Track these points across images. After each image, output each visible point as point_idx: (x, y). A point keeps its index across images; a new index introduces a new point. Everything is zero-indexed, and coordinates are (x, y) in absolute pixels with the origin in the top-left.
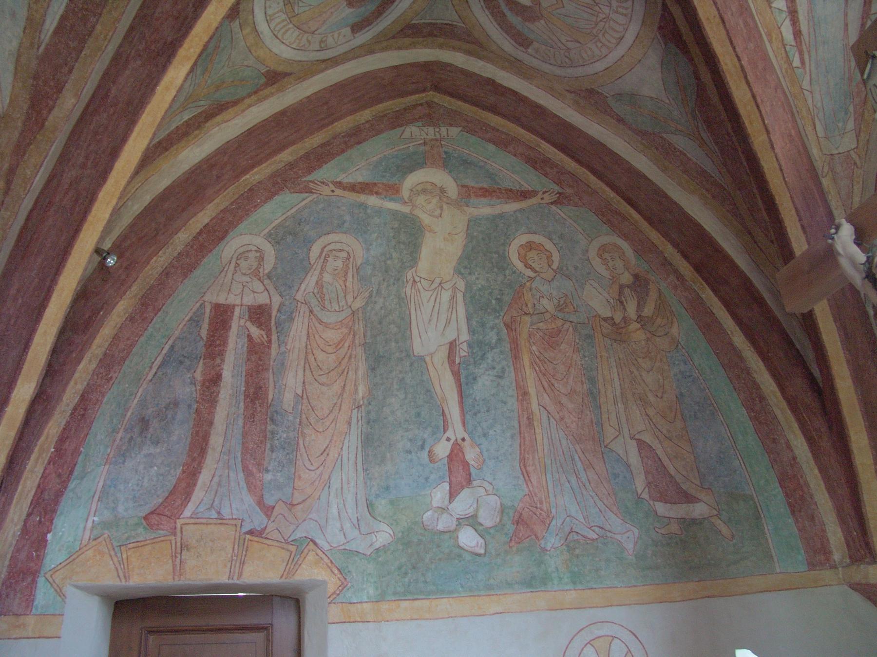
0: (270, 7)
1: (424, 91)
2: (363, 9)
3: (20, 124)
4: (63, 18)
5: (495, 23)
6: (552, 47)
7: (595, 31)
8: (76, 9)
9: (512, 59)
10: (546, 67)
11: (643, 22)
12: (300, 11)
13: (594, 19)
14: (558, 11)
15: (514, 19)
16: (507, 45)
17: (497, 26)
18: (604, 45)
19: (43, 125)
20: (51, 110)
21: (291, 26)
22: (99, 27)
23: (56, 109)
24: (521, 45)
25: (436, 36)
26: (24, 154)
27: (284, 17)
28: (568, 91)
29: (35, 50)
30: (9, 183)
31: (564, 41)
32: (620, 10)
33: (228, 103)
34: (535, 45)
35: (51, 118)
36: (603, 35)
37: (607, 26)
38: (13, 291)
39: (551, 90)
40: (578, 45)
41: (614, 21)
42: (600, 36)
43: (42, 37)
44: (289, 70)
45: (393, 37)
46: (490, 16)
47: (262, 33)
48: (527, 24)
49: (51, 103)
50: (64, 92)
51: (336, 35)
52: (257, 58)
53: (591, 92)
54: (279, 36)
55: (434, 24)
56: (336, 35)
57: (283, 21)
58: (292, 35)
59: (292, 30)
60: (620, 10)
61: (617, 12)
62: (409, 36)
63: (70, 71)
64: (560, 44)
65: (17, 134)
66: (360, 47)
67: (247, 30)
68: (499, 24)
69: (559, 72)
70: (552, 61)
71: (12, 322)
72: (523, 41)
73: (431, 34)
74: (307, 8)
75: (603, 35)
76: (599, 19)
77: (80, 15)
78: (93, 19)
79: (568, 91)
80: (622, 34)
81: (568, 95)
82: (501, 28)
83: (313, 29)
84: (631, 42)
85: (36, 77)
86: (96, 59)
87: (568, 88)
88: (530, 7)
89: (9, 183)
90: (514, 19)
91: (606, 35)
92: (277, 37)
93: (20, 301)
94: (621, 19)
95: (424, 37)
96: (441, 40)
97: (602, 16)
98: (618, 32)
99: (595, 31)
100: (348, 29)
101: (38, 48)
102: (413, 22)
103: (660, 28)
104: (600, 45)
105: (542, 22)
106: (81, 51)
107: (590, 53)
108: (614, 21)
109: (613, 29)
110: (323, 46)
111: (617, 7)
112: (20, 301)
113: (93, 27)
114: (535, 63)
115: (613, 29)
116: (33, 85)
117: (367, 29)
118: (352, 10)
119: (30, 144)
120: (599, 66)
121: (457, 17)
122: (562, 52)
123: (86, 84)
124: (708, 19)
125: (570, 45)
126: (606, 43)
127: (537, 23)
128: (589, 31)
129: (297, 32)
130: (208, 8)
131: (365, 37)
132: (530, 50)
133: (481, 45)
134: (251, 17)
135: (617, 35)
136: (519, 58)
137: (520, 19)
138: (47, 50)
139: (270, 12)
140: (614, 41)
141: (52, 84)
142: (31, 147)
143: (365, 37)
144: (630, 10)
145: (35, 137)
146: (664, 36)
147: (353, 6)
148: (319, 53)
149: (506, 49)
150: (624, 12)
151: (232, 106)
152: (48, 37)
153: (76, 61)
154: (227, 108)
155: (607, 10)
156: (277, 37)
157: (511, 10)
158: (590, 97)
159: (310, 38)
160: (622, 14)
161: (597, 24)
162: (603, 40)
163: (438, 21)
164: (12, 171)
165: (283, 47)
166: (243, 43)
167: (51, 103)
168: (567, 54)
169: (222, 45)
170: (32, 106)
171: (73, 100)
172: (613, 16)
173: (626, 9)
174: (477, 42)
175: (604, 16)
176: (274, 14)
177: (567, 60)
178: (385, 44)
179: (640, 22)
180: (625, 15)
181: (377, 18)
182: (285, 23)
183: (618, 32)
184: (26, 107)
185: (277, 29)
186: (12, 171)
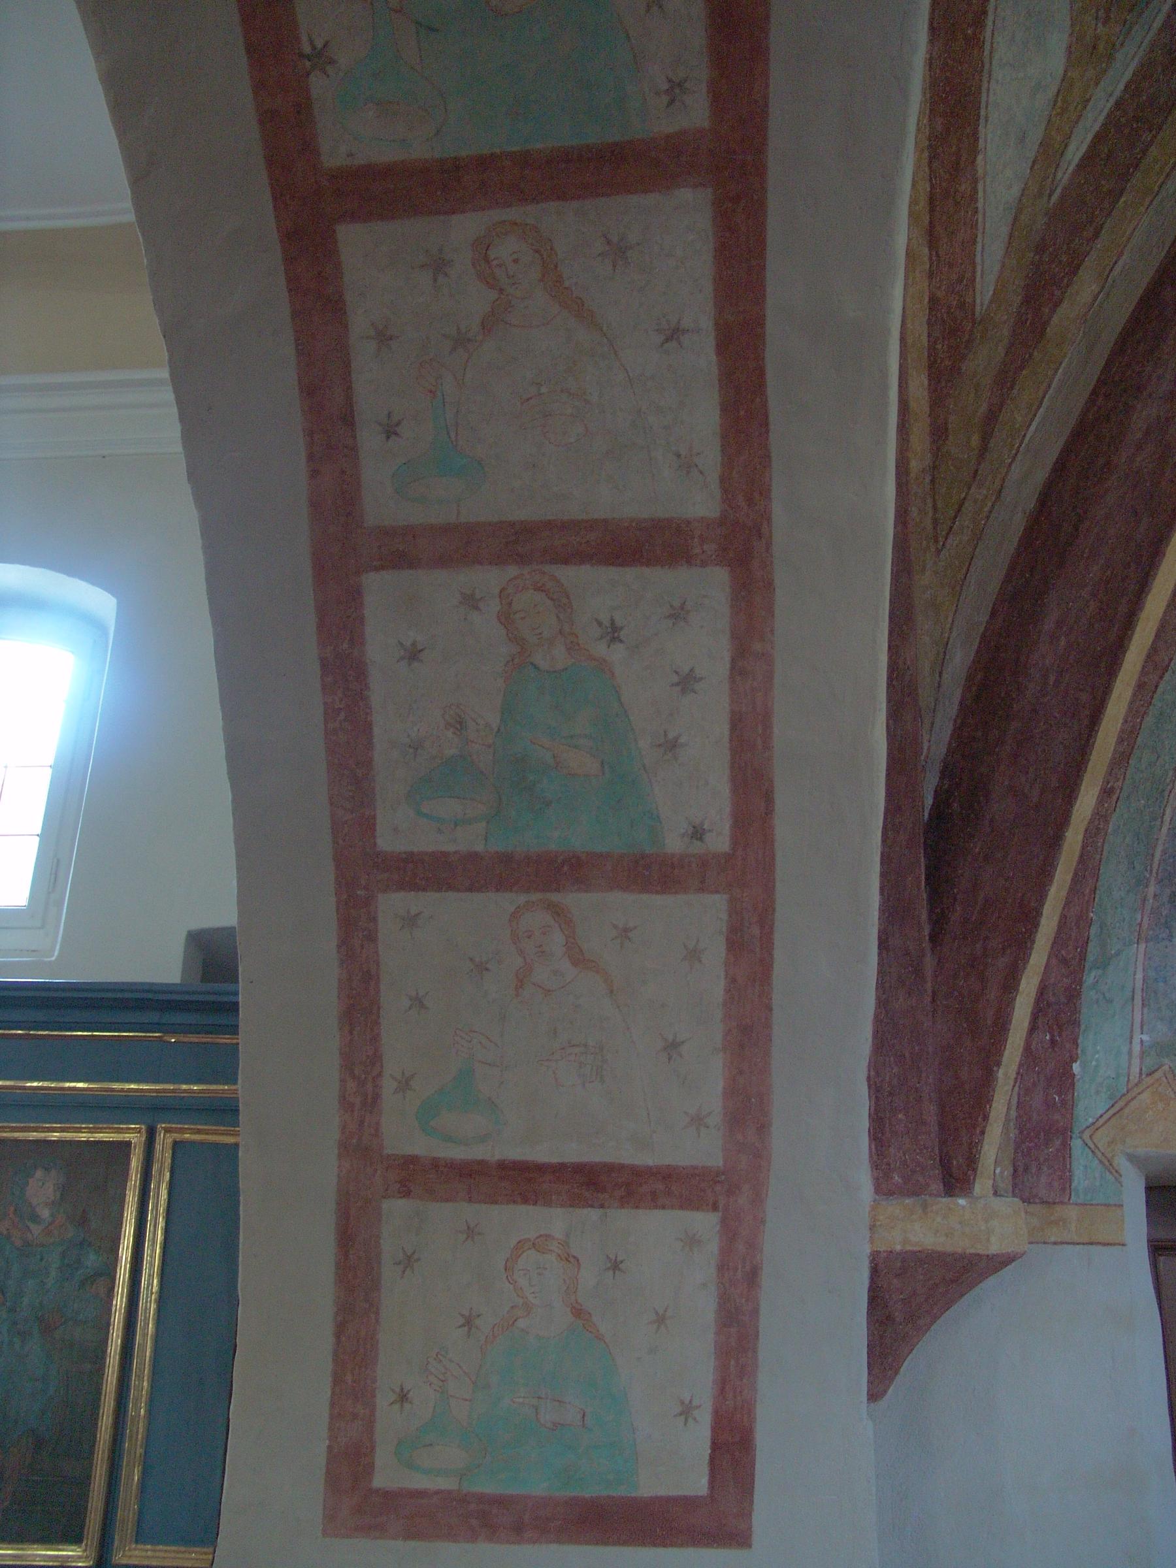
3: (1006, 332)
4: (1099, 138)
8: (1123, 120)
19: (1043, 333)
20: (1057, 305)
22: (1154, 151)
23: (1065, 304)
26: (1012, 387)
29: (1045, 198)
30: (986, 438)
35: (1055, 320)
38: (1049, 625)
43: (1059, 175)
49: (1057, 293)
50: (1080, 273)
63: (1097, 234)
65: (1001, 351)
71: (1052, 678)
77: (1126, 131)
78: (1146, 137)
85: (1040, 248)
86: (1142, 209)
89: (986, 438)
93: (1063, 642)
101: (1050, 196)
106: (1121, 194)
112: (1063, 642)
113: (1144, 152)
116: (1032, 263)
119: (1022, 368)
123: (1121, 254)
138: (1062, 197)
141: (1064, 258)
142: (1024, 372)
145: (1031, 355)
152: (1067, 176)
153: (1109, 214)
164: (992, 418)
167: (1057, 293)
170: (1027, 300)
171: (1095, 288)
184: (1018, 299)
186: (992, 418)
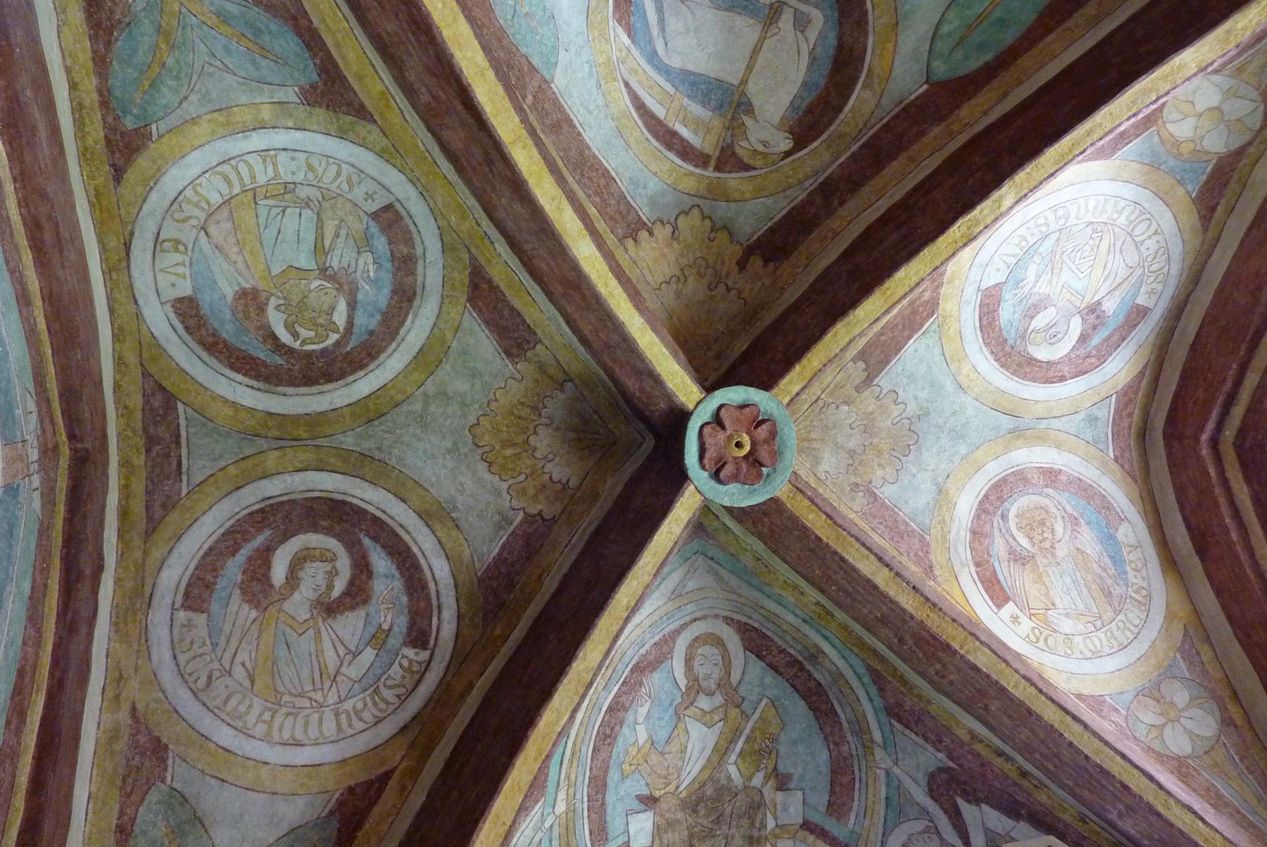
0: (293, 159)
1: (72, 437)
2: (228, 316)
5: (210, 542)
6: (215, 645)
7: (286, 698)
9: (148, 590)
10: (161, 653)
11: (344, 761)
12: (263, 212)
13: (308, 687)
14: (288, 630)
15: (234, 568)
16: (174, 573)
17: (206, 547)
18: (270, 724)
21: (237, 190)
24: (187, 595)
25: (148, 451)
27: (262, 180)
28: (134, 709)
31: (239, 658)
32: (343, 717)
33: (109, 44)
34: (201, 619)
36: (288, 714)
37: (306, 712)
39: (117, 678)
40: (247, 683)
41: (321, 720)
42: (284, 710)
44: (130, 176)
45: (146, 374)
46: (222, 530)
47: (246, 137)
48: (238, 591)
51: (180, 270)
52: (194, 121)
53: (158, 750)
54: (225, 168)
55: (178, 443)
56: (180, 270)
57: (253, 177)
58: (214, 191)
59: (225, 191)
60: (343, 717)
61: (337, 715)
62: (147, 401)
64: (228, 656)
66: (139, 316)
67: (266, 113)
68: (211, 549)
69: (168, 676)
70: (182, 658)
72: (197, 594)
73: (151, 441)
74: (262, 221)
75: (288, 714)
76: (312, 695)
79: (134, 709)
80: (307, 742)
81: (124, 716)
82: (206, 554)
83: (212, 229)
84: (299, 762)
87: (140, 706)
88: (272, 586)
90: (234, 568)
91: (291, 719)
92: (224, 162)
94: (330, 728)
95: (145, 430)
96: (139, 460)
97: (318, 696)
98: (306, 732)
99: (286, 698)
100: (185, 289)
102: (180, 406)
103: (351, 790)
104: (267, 716)
105: (254, 614)
107: (242, 708)
108: (321, 720)
109: (307, 723)
110: (166, 245)
111: (347, 712)
114: (160, 633)
115: (307, 723)
117: (179, 326)
118: (230, 298)
120: (224, 736)
121: (198, 478)
122: (216, 665)
124: (498, 816)
125: (239, 672)
126: (276, 726)
127: (246, 607)
128: (282, 689)
129: (215, 199)
130: (481, 52)
131: (159, 321)
132: (182, 615)
133: (149, 534)
134: (290, 124)
135: (299, 735)
136: (155, 603)
137: (239, 578)
139: (283, 157)
140: (286, 735)
143: (159, 321)
144: (352, 732)
146: (341, 803)
147: (235, 299)
148: (149, 236)
149: (165, 574)
150: (345, 725)
151: (95, 52)
154: (94, 39)
155: (332, 698)
156: (224, 162)
157: (250, 559)
158: (146, 753)
159: (194, 222)
160: (338, 724)
161: (301, 695)
162: (278, 719)
163: (184, 451)
165: (196, 171)
166: (244, 99)
168: (217, 674)
169: (264, 63)
172: (328, 716)
173: (350, 725)
174: (153, 526)
175: (321, 700)
176: (275, 165)
177: (204, 679)
178: (132, 359)
179: (340, 758)
180: (339, 729)
181: (202, 343)
182: (247, 180)
183: (306, 732)
185: (242, 166)
